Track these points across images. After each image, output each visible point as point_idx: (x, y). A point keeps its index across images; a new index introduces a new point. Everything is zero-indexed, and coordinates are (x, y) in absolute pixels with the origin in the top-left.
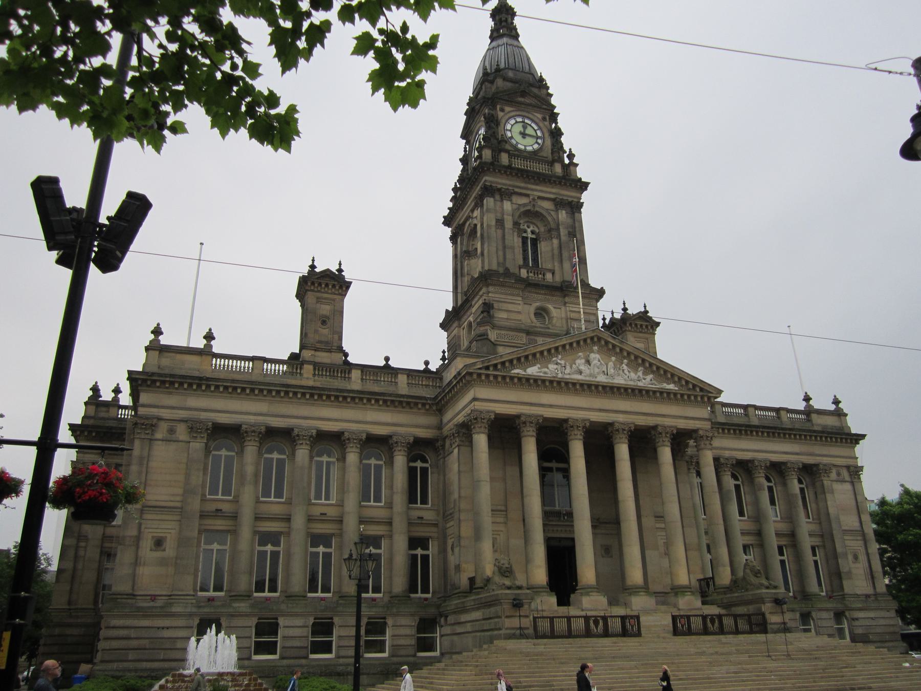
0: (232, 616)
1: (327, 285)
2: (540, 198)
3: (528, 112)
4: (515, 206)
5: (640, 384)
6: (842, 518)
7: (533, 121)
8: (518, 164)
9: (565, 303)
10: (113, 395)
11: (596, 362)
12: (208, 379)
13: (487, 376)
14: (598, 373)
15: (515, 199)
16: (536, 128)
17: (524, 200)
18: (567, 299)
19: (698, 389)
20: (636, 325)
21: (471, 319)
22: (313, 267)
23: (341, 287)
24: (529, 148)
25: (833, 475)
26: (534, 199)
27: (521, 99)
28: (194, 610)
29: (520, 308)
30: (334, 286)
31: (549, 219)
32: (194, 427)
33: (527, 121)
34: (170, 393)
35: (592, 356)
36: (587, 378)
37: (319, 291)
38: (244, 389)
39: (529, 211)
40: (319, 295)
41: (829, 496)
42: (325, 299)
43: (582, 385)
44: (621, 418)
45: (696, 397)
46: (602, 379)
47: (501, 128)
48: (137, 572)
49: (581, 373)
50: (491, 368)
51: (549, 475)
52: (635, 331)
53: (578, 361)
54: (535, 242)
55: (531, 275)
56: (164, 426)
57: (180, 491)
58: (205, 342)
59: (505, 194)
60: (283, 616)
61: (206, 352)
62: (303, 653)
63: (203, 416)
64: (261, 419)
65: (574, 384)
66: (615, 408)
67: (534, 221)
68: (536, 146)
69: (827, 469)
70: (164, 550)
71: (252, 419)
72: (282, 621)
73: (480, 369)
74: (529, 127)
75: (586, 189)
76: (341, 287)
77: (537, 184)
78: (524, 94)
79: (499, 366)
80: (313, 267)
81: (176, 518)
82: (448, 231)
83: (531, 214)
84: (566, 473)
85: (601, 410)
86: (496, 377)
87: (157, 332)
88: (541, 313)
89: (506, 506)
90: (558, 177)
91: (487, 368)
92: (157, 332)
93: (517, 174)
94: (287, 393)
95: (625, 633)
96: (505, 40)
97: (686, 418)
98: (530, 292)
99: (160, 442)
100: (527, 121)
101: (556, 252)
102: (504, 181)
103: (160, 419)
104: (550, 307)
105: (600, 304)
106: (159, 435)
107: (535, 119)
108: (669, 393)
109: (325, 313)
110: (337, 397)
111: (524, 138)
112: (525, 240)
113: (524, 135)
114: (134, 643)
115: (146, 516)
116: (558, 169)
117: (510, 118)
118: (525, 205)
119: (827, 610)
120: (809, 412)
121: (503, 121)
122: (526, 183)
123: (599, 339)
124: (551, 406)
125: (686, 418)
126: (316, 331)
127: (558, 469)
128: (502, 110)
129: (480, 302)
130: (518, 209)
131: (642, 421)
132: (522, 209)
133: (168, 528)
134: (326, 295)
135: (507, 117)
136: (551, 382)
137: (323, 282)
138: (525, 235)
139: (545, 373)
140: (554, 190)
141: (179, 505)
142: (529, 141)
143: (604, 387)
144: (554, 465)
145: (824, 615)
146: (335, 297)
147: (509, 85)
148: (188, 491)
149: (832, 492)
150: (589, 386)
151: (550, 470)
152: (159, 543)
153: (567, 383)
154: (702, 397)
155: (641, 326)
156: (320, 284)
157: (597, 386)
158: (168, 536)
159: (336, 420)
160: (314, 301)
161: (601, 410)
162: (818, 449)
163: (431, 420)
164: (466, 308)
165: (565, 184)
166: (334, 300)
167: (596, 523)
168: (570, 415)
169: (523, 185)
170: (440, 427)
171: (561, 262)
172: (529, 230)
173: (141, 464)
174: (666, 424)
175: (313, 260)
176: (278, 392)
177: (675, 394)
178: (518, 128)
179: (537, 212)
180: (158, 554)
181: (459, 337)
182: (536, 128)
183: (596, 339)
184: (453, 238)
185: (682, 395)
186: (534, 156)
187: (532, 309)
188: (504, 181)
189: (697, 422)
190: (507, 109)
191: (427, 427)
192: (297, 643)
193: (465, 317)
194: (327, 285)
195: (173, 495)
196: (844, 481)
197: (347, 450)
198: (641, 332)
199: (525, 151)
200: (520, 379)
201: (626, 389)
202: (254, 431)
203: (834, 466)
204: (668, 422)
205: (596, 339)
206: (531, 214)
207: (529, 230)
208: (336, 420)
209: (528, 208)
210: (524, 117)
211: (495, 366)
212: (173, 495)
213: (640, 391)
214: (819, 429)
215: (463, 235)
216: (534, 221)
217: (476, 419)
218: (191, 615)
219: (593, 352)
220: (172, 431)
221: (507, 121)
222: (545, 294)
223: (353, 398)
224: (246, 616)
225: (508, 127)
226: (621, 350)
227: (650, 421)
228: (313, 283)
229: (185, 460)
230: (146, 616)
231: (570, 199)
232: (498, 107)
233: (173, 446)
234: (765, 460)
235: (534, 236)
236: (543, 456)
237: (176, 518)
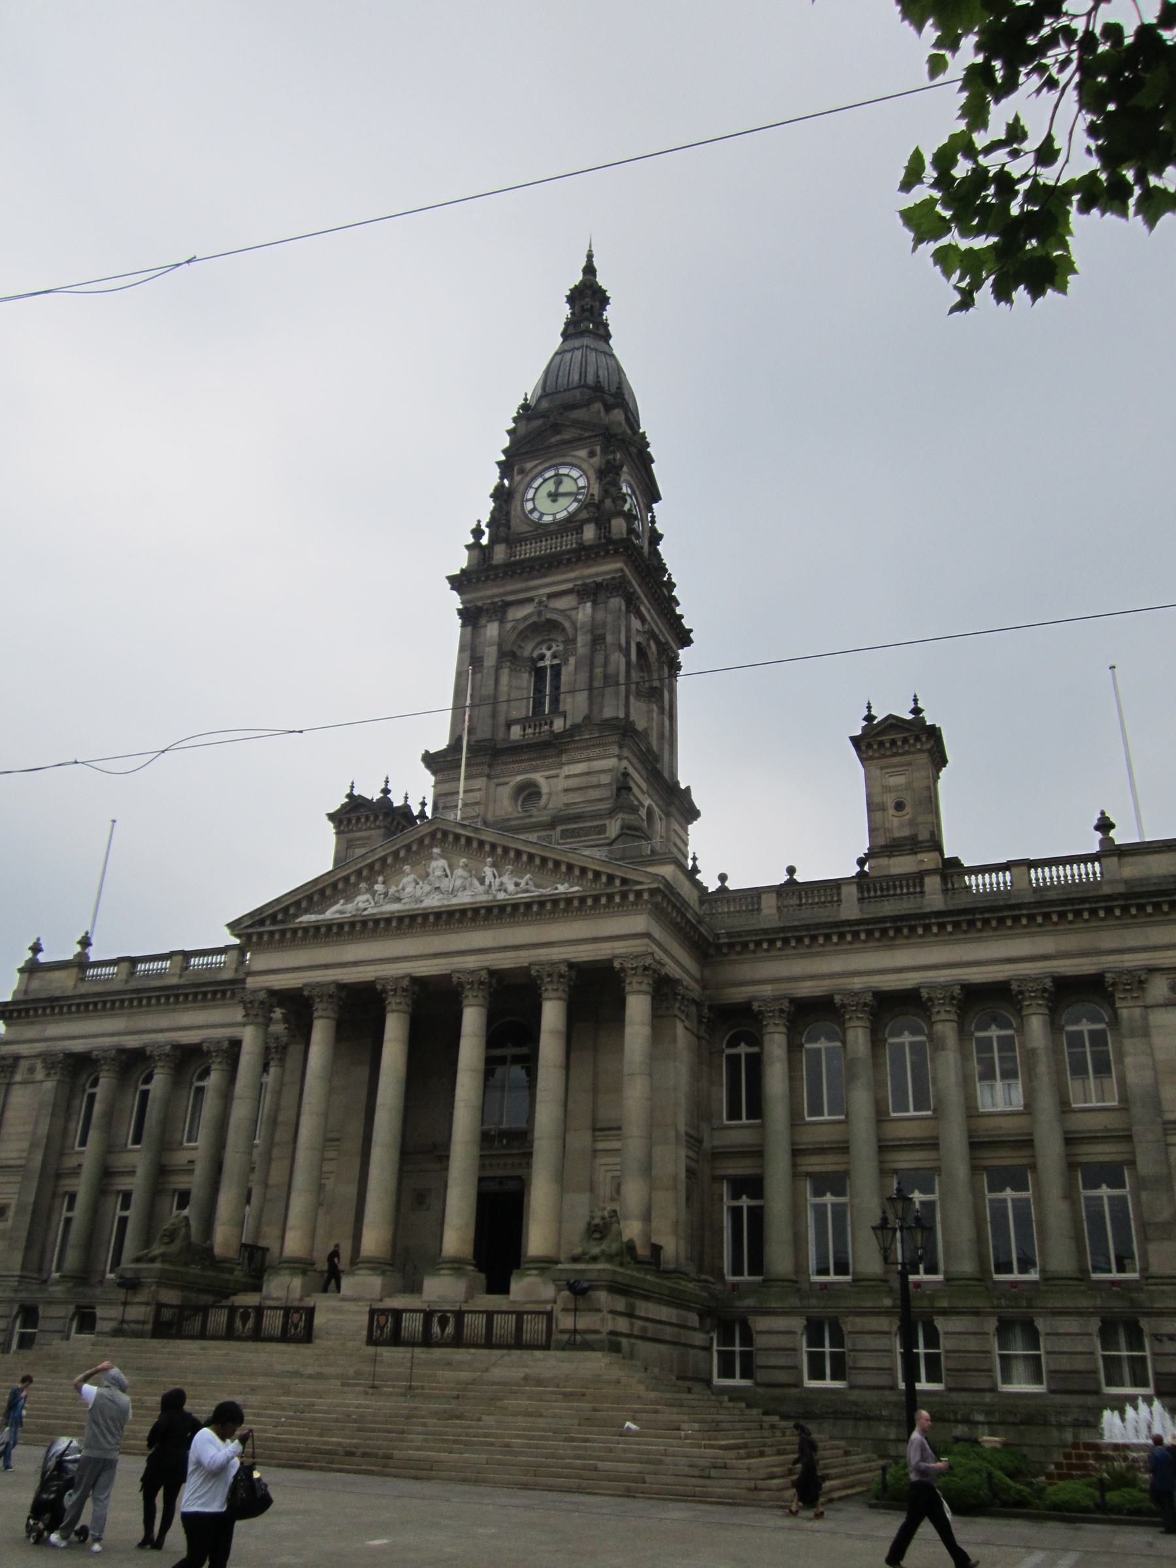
0: (50, 1303)
1: (358, 819)
2: (551, 596)
3: (564, 456)
4: (509, 626)
5: (501, 896)
7: (572, 465)
9: (561, 765)
11: (439, 873)
12: (57, 999)
13: (260, 935)
14: (428, 894)
15: (517, 613)
16: (540, 480)
17: (528, 609)
18: (564, 758)
19: (618, 882)
20: (881, 744)
25: (1159, 988)
26: (540, 603)
27: (554, 439)
28: (12, 1295)
30: (367, 819)
31: (567, 625)
32: (50, 1061)
33: (563, 471)
35: (434, 864)
36: (407, 907)
37: (352, 831)
38: (95, 1004)
39: (534, 623)
40: (351, 835)
41: (1129, 1044)
43: (401, 919)
44: (471, 962)
45: (610, 897)
46: (433, 902)
47: (516, 503)
49: (399, 900)
50: (268, 922)
51: (499, 1070)
52: (884, 756)
53: (405, 880)
54: (556, 670)
55: (529, 731)
56: (24, 1064)
57: (25, 1145)
58: (78, 949)
59: (499, 610)
60: (103, 1304)
61: (81, 963)
65: (388, 921)
66: (463, 947)
67: (552, 636)
69: (1138, 981)
72: (100, 1312)
73: (250, 926)
74: (565, 479)
77: (544, 576)
78: (556, 428)
79: (280, 917)
83: (545, 628)
84: (530, 1063)
85: (436, 955)
86: (272, 933)
87: (36, 949)
88: (528, 793)
90: (591, 547)
92: (36, 949)
93: (505, 574)
94: (140, 1000)
95: (284, 1337)
96: (586, 341)
97: (595, 940)
98: (504, 764)
100: (563, 471)
102: (489, 592)
103: (17, 1058)
104: (538, 777)
107: (575, 461)
108: (555, 902)
110: (196, 995)
111: (554, 501)
112: (539, 674)
113: (554, 496)
116: (589, 533)
117: (534, 479)
118: (525, 618)
119: (1079, 1313)
120: (1110, 851)
121: (522, 488)
122: (527, 580)
123: (445, 834)
124: (355, 964)
125: (595, 940)
127: (516, 1060)
128: (522, 471)
130: (514, 628)
131: (505, 961)
132: (522, 626)
134: (358, 834)
135: (528, 479)
136: (352, 924)
137: (353, 815)
138: (541, 664)
139: (341, 912)
140: (572, 575)
141: (22, 1162)
142: (563, 502)
143: (438, 915)
144: (510, 1051)
145: (1070, 1325)
146: (373, 832)
147: (539, 422)
148: (33, 1145)
149: (1145, 1032)
150: (413, 918)
151: (502, 1060)
153: (377, 922)
154: (624, 896)
155: (893, 742)
156: (349, 821)
157: (425, 916)
161: (436, 955)
162: (1109, 939)
165: (588, 557)
166: (368, 838)
167: (440, 1153)
168: (380, 974)
169: (519, 586)
172: (548, 654)
174: (556, 957)
176: (131, 1000)
177: (569, 901)
178: (550, 486)
179: (549, 621)
182: (540, 480)
183: (439, 835)
185: (582, 900)
186: (571, 524)
187: (505, 792)
188: (489, 592)
189: (616, 944)
190: (529, 465)
194: (358, 819)
198: (894, 755)
199: (555, 523)
200: (306, 930)
201: (476, 910)
202: (105, 1058)
203: (1152, 970)
205: (439, 835)
206: (545, 628)
207: (548, 654)
209: (534, 619)
210: (556, 466)
213: (502, 908)
214: (1121, 888)
216: (552, 636)
218: (11, 1301)
219: (431, 858)
220: (32, 1070)
221: (529, 486)
222: (530, 760)
223: (215, 993)
224: (60, 1303)
225: (530, 494)
226: (481, 843)
231: (599, 579)
232: (516, 468)
233: (30, 1088)
234: (946, 986)
235: (556, 662)
236: (495, 1037)
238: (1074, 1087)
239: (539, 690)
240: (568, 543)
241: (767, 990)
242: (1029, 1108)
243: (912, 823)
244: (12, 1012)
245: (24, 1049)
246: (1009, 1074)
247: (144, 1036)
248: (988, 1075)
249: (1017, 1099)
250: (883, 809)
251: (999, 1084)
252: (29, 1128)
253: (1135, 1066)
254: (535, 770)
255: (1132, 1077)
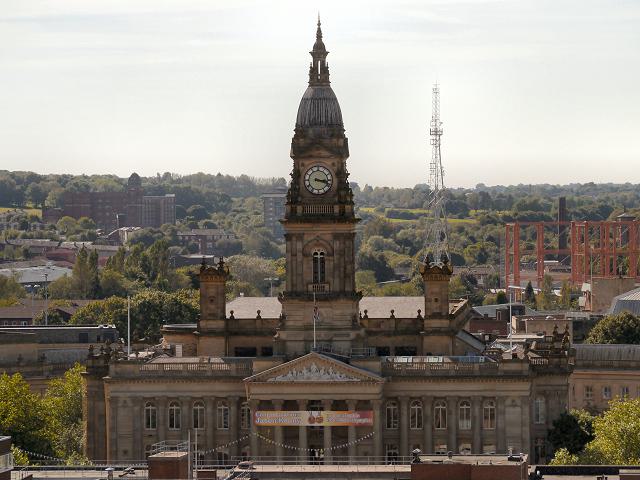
6: (508, 429)
8: (311, 210)
24: (322, 191)
25: (508, 402)
63: (138, 394)
64: (164, 394)
68: (326, 188)
69: (503, 399)
71: (160, 394)
106: (120, 405)
109: (212, 294)
126: (207, 309)
149: (504, 413)
190: (306, 162)
196: (516, 406)
203: (507, 397)
204: (354, 397)
227: (343, 397)
238: (484, 425)
239: (315, 267)
240: (323, 209)
241: (403, 394)
242: (473, 428)
243: (441, 308)
246: (468, 418)
248: (462, 418)
249: (470, 424)
250: (430, 301)
251: (465, 421)
253: (500, 421)
255: (500, 425)
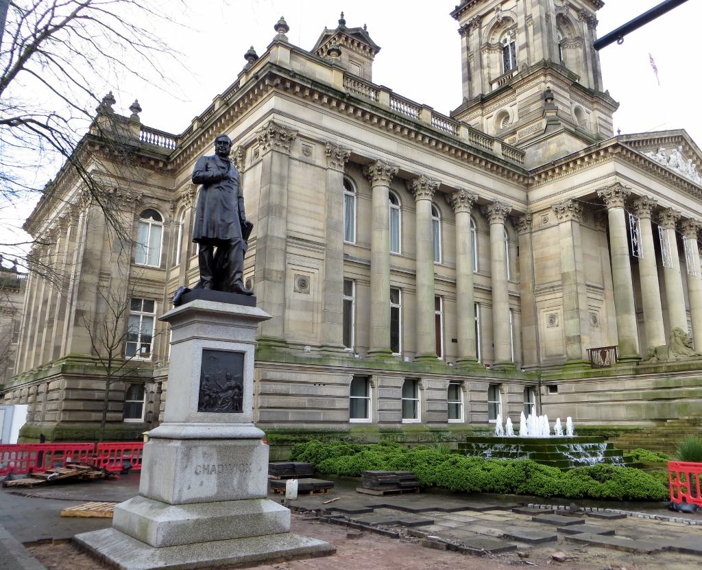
1: (359, 45)
10: (131, 113)
21: (507, 108)
22: (342, 22)
23: (370, 51)
29: (568, 103)
31: (576, 28)
32: (332, 152)
34: (306, 105)
36: (681, 173)
40: (351, 53)
42: (356, 59)
48: (287, 316)
56: (299, 143)
62: (444, 417)
63: (340, 141)
64: (391, 158)
70: (308, 293)
75: (602, 6)
76: (370, 51)
80: (342, 22)
81: (322, 256)
82: (457, 25)
89: (604, 285)
91: (626, 143)
99: (297, 162)
101: (582, 59)
104: (584, 108)
105: (614, 115)
106: (296, 154)
114: (292, 401)
115: (290, 250)
118: (560, 8)
129: (536, 90)
133: (312, 266)
134: (356, 55)
137: (357, 40)
146: (365, 59)
148: (331, 227)
152: (303, 284)
156: (353, 42)
158: (312, 276)
159: (454, 176)
160: (347, 58)
163: (519, 194)
164: (499, 97)
166: (363, 63)
170: (527, 202)
171: (587, 70)
173: (282, 185)
175: (342, 15)
180: (303, 297)
181: (482, 125)
184: (465, 31)
191: (519, 201)
192: (440, 407)
193: (495, 106)
194: (359, 45)
195: (314, 228)
197: (456, 211)
208: (454, 176)
211: (631, 143)
212: (314, 228)
215: (480, 28)
217: (617, 193)
220: (307, 152)
228: (347, 39)
229: (323, 190)
230: (303, 369)
233: (310, 170)
237: (322, 256)
244: (294, 85)
245: (304, 129)
247: (414, 165)
252: (321, 210)
254: (583, 104)
